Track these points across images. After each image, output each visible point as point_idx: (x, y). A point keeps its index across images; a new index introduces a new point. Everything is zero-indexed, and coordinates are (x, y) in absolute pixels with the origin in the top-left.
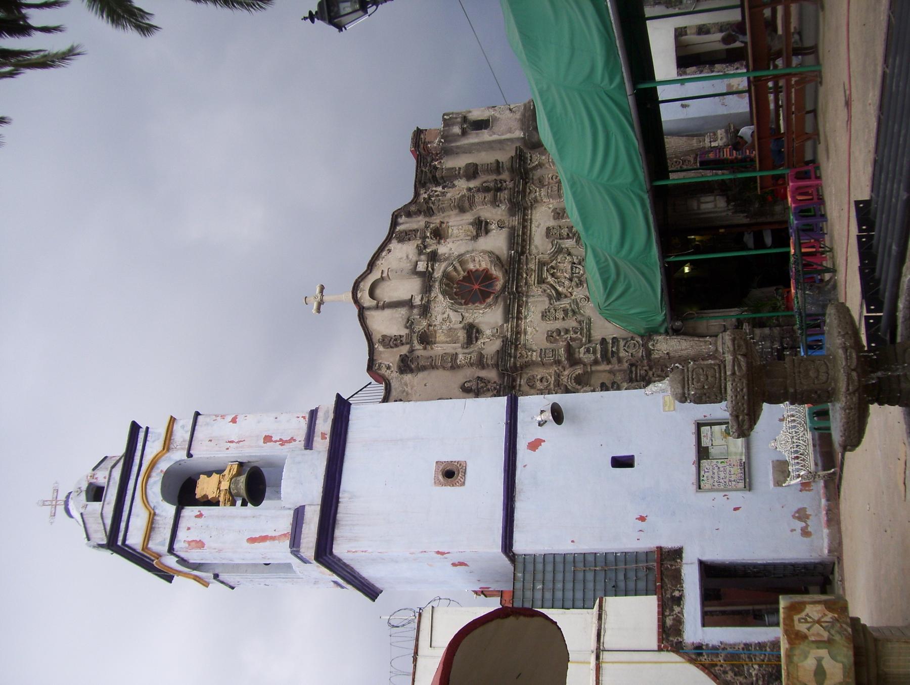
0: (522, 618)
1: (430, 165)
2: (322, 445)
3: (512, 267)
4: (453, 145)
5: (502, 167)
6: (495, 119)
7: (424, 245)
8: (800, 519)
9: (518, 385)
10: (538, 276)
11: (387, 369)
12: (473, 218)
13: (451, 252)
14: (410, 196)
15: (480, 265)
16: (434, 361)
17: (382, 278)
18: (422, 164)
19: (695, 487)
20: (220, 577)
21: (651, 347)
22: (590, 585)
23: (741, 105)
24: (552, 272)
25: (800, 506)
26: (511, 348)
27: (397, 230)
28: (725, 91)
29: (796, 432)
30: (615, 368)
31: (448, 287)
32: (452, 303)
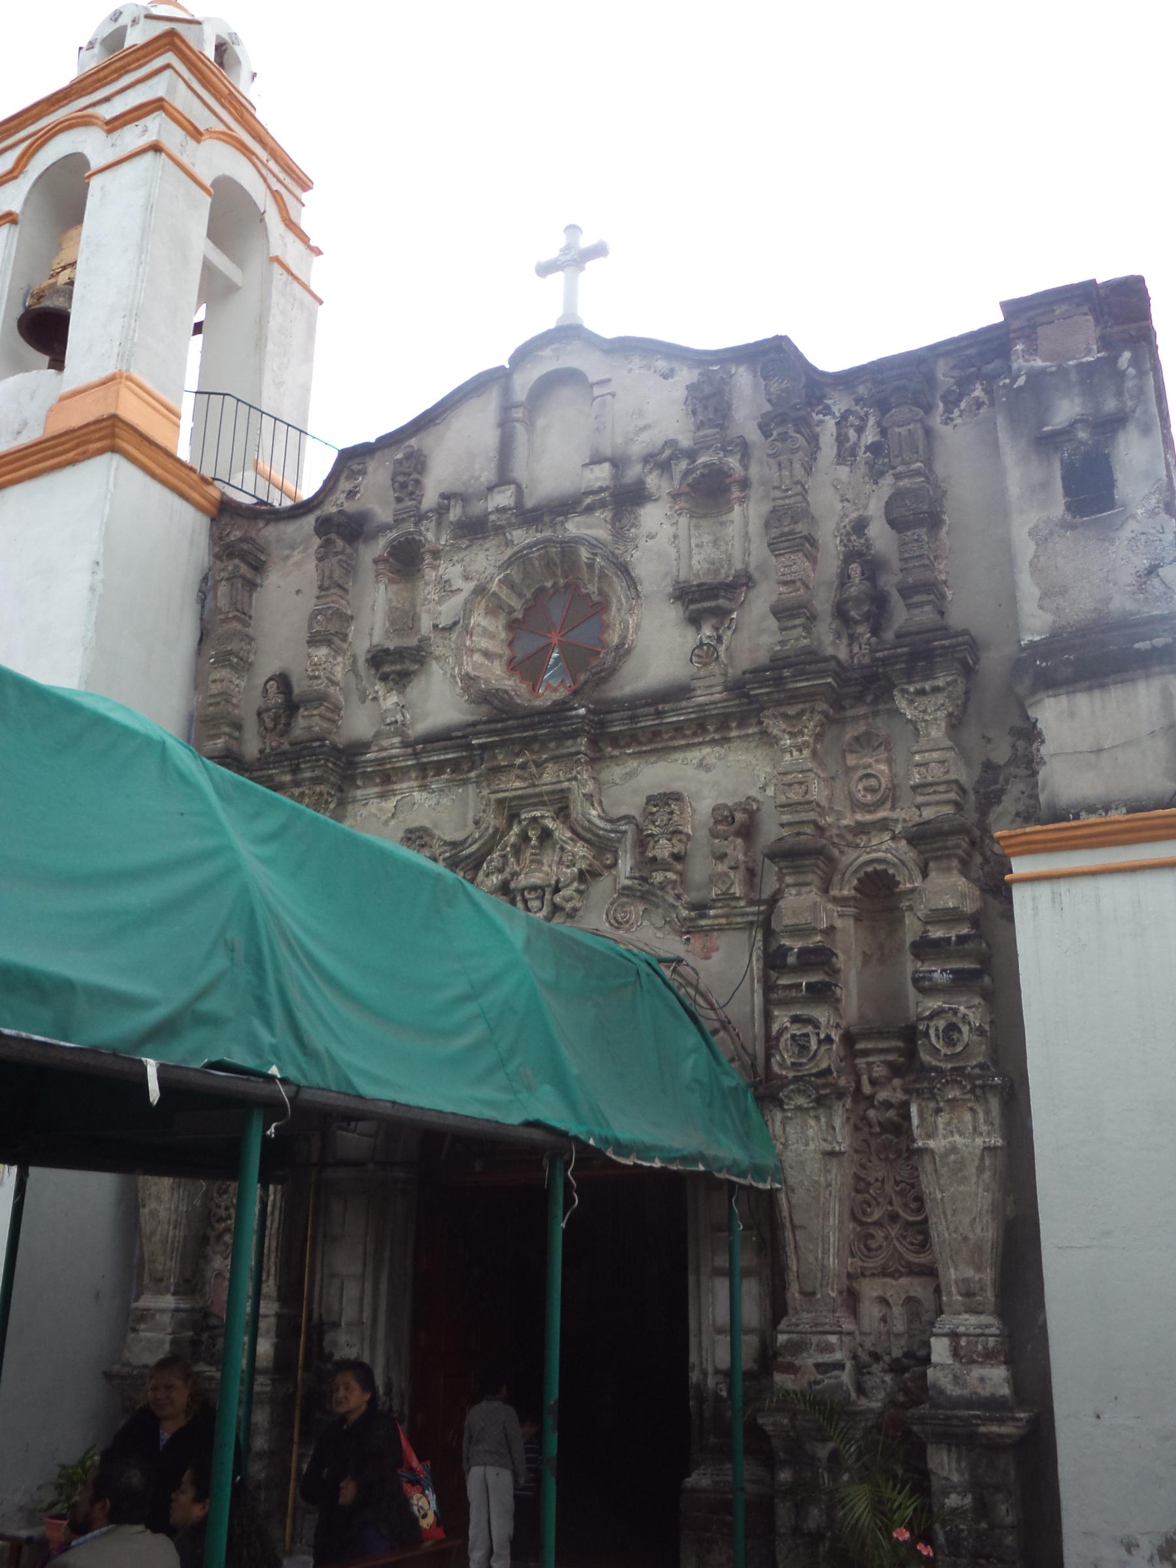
10: (520, 797)
12: (752, 568)
13: (642, 543)
26: (313, 769)
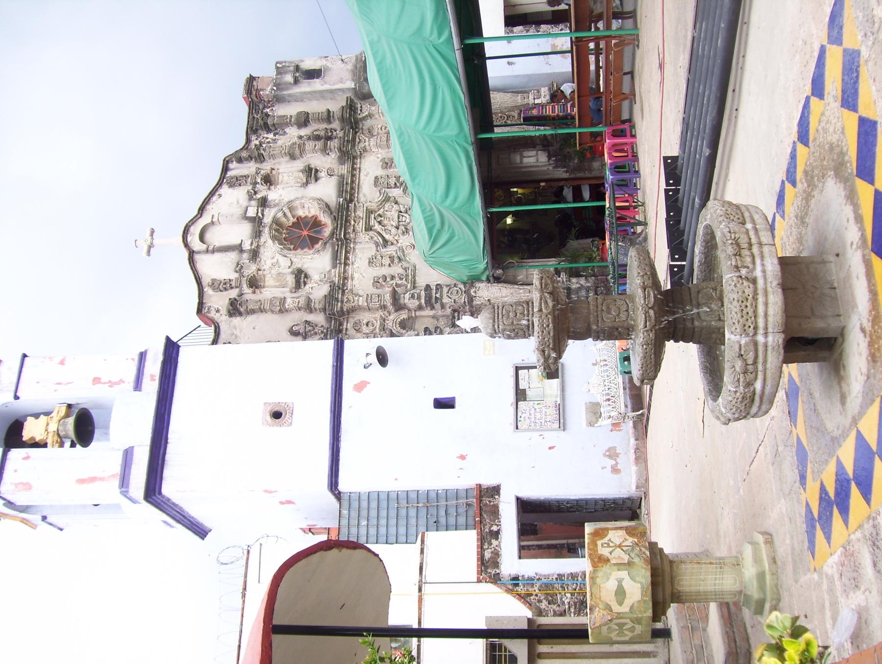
0: (344, 550)
1: (262, 112)
2: (151, 387)
3: (340, 214)
4: (284, 93)
5: (333, 116)
6: (327, 69)
7: (254, 191)
8: (610, 457)
9: (344, 329)
10: (366, 223)
11: (217, 312)
13: (281, 198)
14: (242, 142)
15: (309, 212)
16: (262, 305)
17: (213, 223)
18: (254, 111)
19: (513, 427)
20: (48, 518)
21: (472, 294)
22: (413, 521)
23: (564, 65)
24: (379, 220)
25: (611, 445)
26: (338, 293)
27: (228, 175)
28: (549, 51)
29: (608, 376)
30: (438, 314)
31: (278, 233)
32: (281, 248)
